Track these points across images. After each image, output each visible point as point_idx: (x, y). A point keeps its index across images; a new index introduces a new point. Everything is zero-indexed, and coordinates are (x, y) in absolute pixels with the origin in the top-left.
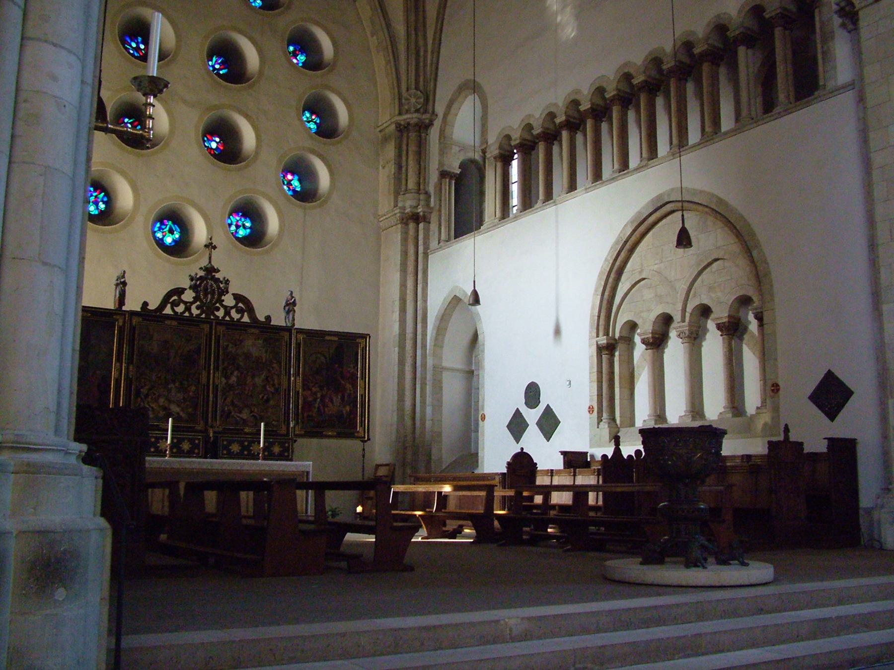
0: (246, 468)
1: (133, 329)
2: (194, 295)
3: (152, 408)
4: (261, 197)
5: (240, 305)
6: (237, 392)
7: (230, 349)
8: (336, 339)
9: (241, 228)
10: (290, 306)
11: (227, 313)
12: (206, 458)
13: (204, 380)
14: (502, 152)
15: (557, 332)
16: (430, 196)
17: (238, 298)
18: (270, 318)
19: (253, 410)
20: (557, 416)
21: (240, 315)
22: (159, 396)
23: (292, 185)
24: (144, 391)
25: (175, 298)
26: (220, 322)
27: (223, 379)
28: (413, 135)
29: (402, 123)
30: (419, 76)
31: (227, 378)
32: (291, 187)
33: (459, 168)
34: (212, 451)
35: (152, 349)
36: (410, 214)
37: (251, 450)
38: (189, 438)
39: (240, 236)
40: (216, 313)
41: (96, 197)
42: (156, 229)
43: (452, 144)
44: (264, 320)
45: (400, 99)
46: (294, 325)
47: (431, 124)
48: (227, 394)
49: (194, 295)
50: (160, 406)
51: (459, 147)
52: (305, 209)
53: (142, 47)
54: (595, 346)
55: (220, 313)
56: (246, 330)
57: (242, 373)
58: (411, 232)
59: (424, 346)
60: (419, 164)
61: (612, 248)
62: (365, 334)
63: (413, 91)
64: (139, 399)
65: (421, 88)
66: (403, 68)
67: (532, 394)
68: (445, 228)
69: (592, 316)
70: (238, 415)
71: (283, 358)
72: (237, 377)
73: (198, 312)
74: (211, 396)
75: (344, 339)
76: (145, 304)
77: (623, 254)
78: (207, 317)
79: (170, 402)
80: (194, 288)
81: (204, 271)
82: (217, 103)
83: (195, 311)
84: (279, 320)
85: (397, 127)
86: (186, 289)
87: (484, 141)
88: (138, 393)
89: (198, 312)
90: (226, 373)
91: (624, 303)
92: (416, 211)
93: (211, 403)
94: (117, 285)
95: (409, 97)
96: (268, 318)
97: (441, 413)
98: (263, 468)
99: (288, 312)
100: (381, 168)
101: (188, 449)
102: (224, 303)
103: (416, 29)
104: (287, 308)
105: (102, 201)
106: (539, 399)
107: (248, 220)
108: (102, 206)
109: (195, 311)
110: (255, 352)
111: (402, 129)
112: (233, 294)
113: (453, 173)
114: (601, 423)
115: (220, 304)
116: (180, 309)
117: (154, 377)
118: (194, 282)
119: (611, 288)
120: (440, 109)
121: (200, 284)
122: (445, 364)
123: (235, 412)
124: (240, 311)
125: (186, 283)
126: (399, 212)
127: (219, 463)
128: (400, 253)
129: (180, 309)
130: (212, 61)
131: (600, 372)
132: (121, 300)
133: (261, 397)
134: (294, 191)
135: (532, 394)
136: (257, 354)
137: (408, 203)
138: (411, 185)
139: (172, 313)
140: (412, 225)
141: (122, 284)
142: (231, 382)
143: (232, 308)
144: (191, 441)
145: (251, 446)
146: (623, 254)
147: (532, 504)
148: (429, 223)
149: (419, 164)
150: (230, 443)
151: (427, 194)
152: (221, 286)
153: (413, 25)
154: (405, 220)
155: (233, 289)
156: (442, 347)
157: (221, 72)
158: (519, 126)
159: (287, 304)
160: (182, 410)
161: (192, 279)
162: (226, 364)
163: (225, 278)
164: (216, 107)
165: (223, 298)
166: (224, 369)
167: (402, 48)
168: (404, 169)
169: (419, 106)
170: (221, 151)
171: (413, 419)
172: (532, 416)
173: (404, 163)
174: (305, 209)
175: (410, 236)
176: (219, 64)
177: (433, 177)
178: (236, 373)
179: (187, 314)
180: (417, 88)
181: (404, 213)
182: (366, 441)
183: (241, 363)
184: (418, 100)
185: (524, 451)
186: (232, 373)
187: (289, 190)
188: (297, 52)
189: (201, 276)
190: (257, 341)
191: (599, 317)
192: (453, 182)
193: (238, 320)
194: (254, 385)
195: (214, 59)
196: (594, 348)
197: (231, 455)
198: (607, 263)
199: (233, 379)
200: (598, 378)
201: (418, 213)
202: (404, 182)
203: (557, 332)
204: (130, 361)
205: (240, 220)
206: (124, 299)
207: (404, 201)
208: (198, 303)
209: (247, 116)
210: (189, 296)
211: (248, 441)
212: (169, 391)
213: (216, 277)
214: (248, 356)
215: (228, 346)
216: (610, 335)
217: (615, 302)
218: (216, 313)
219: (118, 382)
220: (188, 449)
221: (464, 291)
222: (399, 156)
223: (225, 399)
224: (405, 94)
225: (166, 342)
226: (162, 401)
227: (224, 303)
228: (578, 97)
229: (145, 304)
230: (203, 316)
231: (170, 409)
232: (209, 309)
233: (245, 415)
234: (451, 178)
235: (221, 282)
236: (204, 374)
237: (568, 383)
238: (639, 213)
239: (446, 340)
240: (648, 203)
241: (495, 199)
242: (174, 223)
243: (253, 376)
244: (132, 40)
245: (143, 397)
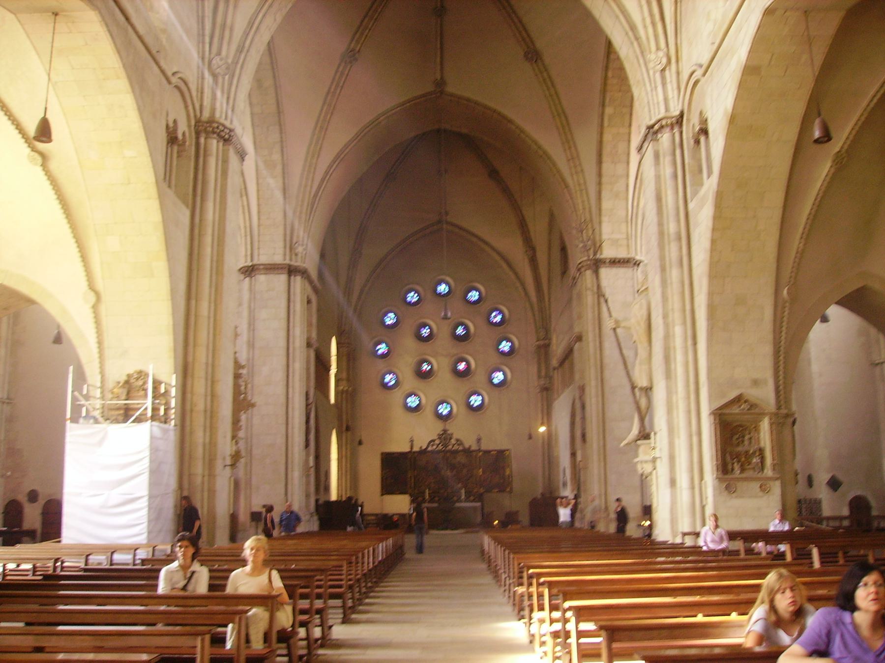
10: (479, 440)
17: (457, 440)
55: (450, 447)
76: (421, 447)
84: (474, 447)
109: (440, 447)
111: (539, 347)
129: (435, 447)
132: (412, 447)
140: (545, 393)
141: (412, 441)
155: (455, 436)
209: (471, 355)
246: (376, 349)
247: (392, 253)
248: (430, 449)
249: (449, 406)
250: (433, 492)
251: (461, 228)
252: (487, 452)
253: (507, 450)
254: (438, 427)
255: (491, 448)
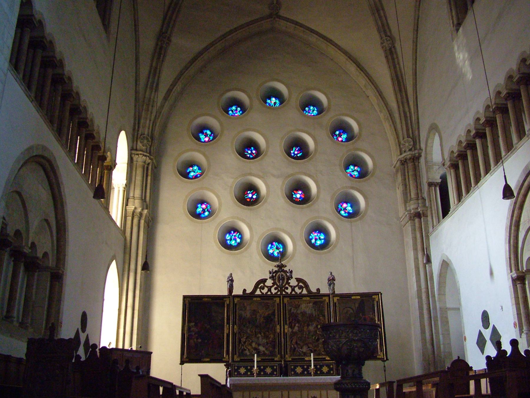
0: (268, 382)
1: (235, 305)
2: (273, 282)
3: (248, 349)
4: (239, 221)
5: (301, 284)
6: (299, 336)
7: (292, 311)
8: (359, 297)
9: (318, 240)
10: (332, 281)
11: (293, 290)
12: (280, 376)
13: (278, 331)
14: (452, 162)
15: (491, 273)
16: (426, 200)
17: (299, 280)
18: (320, 290)
19: (309, 346)
20: (499, 332)
21: (301, 290)
22: (252, 342)
23: (347, 210)
24: (243, 340)
25: (262, 285)
26: (287, 296)
27: (290, 329)
28: (410, 165)
29: (403, 159)
30: (409, 130)
31: (291, 327)
32: (346, 211)
33: (440, 178)
34: (284, 372)
35: (247, 316)
36: (414, 213)
37: (309, 371)
38: (301, 365)
39: (318, 245)
40: (286, 290)
41: (235, 236)
42: (269, 248)
43: (433, 165)
44: (316, 291)
45: (400, 145)
46: (334, 292)
47: (420, 156)
48: (293, 337)
49: (273, 282)
50: (252, 348)
51: (438, 166)
52: (351, 222)
53: (254, 152)
54: (511, 279)
55: (289, 291)
56: (273, 299)
57: (301, 325)
58: (417, 225)
59: (434, 296)
60: (416, 182)
61: (509, 209)
62: (377, 292)
63: (406, 139)
64: (241, 345)
65: (411, 136)
66: (399, 126)
67: (485, 318)
68: (436, 219)
69: (506, 259)
70: (301, 350)
71: (326, 314)
72: (298, 326)
73: (276, 291)
74: (283, 339)
75: (365, 297)
76: (245, 290)
77: (516, 212)
78: (281, 294)
79: (259, 345)
80: (272, 278)
81: (277, 267)
82: (292, 172)
83: (274, 291)
84: (325, 290)
85: (400, 163)
86: (267, 279)
87: (443, 159)
88: (240, 341)
89: (276, 291)
90: (291, 325)
91: (525, 246)
92: (417, 211)
93: (283, 344)
94: (228, 281)
95: (405, 143)
96: (318, 290)
97: (450, 339)
98: (310, 381)
99: (330, 285)
100: (397, 189)
101: (270, 372)
102: (290, 284)
103: (402, 103)
104: (329, 283)
105: (238, 237)
106: (489, 321)
107: (322, 234)
108: (238, 240)
109: (274, 291)
110: (308, 311)
111: (404, 162)
112: (296, 278)
113: (436, 182)
114: (522, 334)
115: (288, 285)
116: (265, 291)
117: (249, 332)
118: (272, 274)
119: (514, 236)
120: (423, 146)
121: (276, 275)
122: (448, 306)
123: (299, 348)
124: (301, 288)
125: (267, 276)
126: (408, 214)
127: (270, 379)
128: (411, 239)
129: (265, 291)
130: (292, 150)
131: (516, 298)
133: (314, 338)
134: (349, 213)
135: (485, 318)
136: (309, 312)
137: (412, 206)
138: (413, 196)
139: (261, 294)
140: (417, 220)
141: (231, 281)
142: (294, 330)
143: (295, 287)
144: (272, 367)
145: (328, 371)
146: (516, 212)
147: (468, 395)
148: (427, 216)
149: (416, 182)
150: (295, 367)
151: (423, 199)
152: (288, 274)
153: (400, 100)
154: (412, 218)
155: (294, 276)
156: (444, 295)
157: (299, 155)
158: (456, 144)
159: (329, 280)
160: (266, 349)
161: (270, 273)
162: (291, 320)
163: (289, 270)
164: (292, 175)
165: (289, 281)
166: (290, 323)
167: (396, 115)
168: (408, 187)
169: (411, 147)
170: (303, 198)
171: (432, 344)
172: (487, 334)
173: (407, 183)
174: (351, 223)
175: (416, 227)
176: (297, 151)
177: (425, 187)
178: (297, 325)
179: (269, 293)
180: (408, 136)
181: (411, 214)
182: (385, 361)
183: (300, 319)
184: (409, 144)
185: (460, 358)
186: (295, 326)
187: (345, 213)
188: (341, 134)
189: (275, 271)
190: (309, 305)
191: (510, 258)
192: (438, 188)
193: (300, 293)
194: (310, 332)
195: (294, 149)
196: (510, 280)
197: (296, 374)
198: (508, 220)
199: (296, 328)
200: (515, 301)
201: (419, 212)
202: (409, 195)
203: (491, 273)
204: (234, 323)
205: (317, 235)
206: (232, 290)
207: (409, 206)
208: (275, 286)
209: (310, 176)
210: (269, 283)
211: (307, 365)
212: (258, 338)
213: (285, 270)
214: (304, 314)
215: (291, 309)
216: (520, 270)
217: (519, 246)
218: (286, 290)
219: (228, 335)
220: (270, 372)
221: (447, 256)
222: (405, 179)
223: (292, 341)
224: (402, 142)
225: (254, 310)
226: (254, 345)
227: (290, 284)
228: (478, 116)
229: (245, 290)
230: (279, 293)
231: (259, 349)
232: (281, 288)
233: (305, 349)
234: (435, 186)
235: (288, 273)
236: (278, 327)
237: (500, 308)
238: (518, 181)
239: (447, 290)
240: (521, 173)
241: (453, 192)
242: (279, 243)
243: (308, 325)
244: (248, 150)
245: (243, 343)
246: (188, 171)
247: (210, 48)
248: (258, 292)
249: (280, 246)
250: (263, 360)
251: (296, 23)
252: (345, 297)
253: (377, 294)
254: (272, 266)
255: (352, 290)
